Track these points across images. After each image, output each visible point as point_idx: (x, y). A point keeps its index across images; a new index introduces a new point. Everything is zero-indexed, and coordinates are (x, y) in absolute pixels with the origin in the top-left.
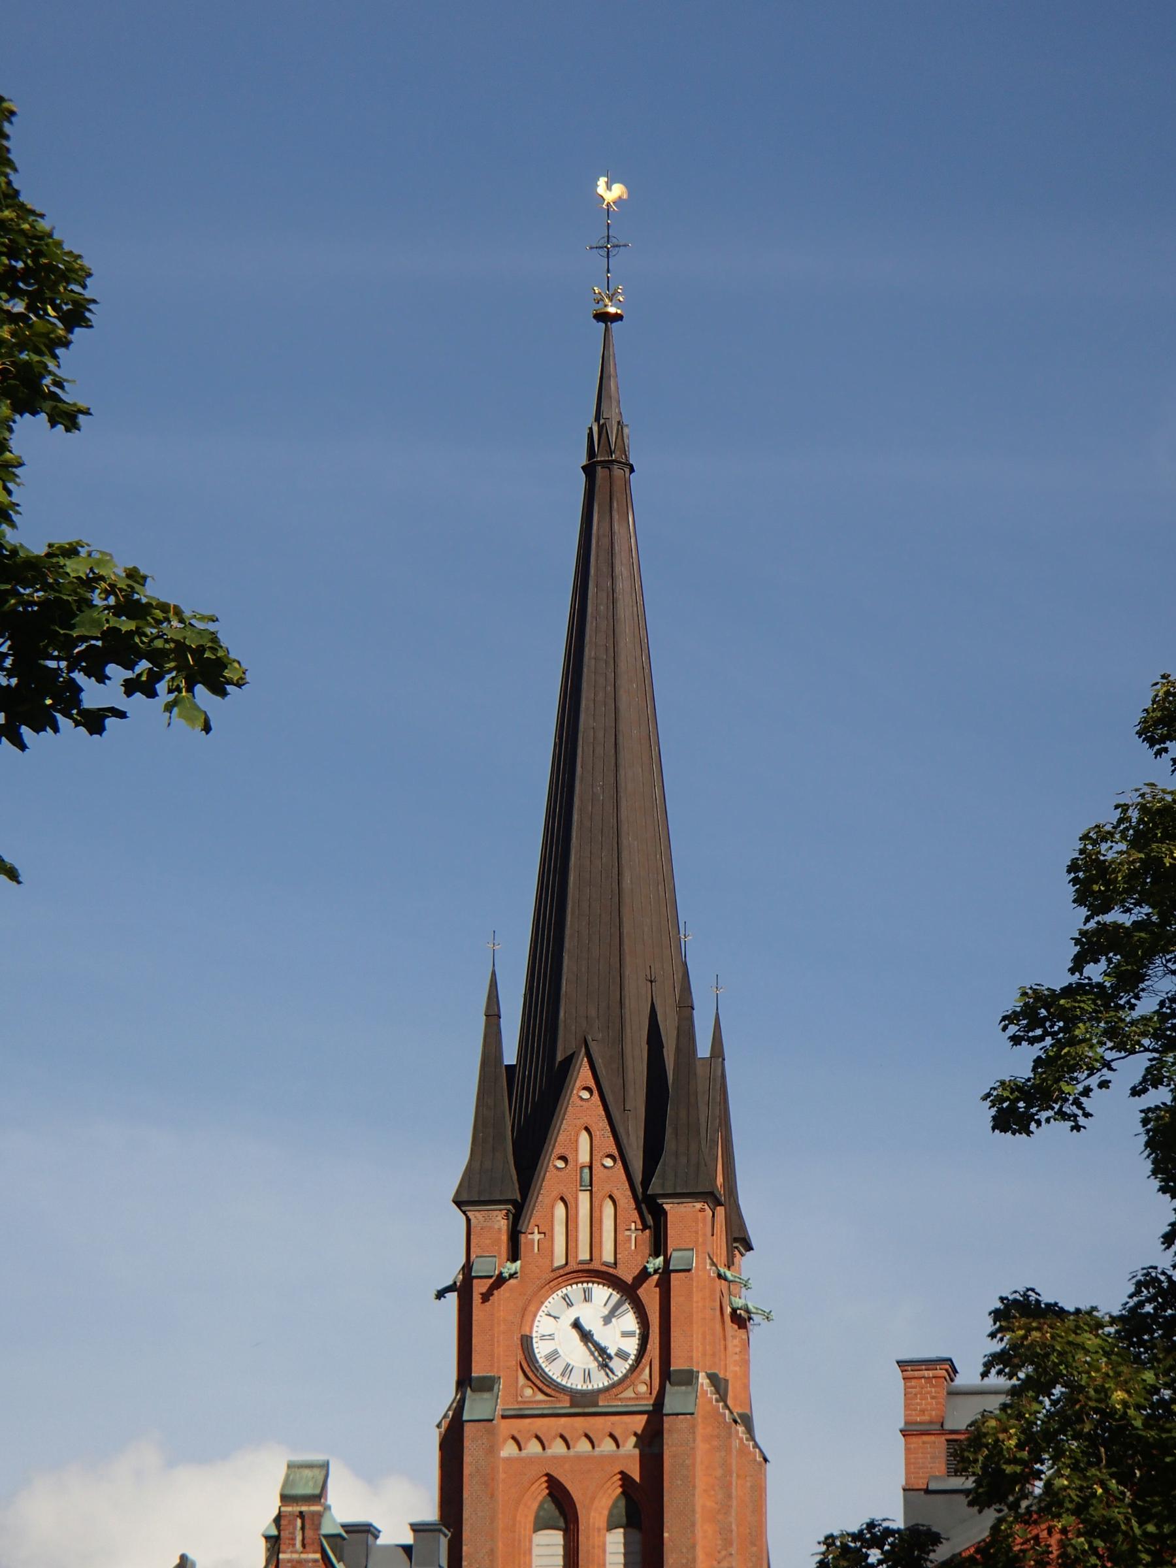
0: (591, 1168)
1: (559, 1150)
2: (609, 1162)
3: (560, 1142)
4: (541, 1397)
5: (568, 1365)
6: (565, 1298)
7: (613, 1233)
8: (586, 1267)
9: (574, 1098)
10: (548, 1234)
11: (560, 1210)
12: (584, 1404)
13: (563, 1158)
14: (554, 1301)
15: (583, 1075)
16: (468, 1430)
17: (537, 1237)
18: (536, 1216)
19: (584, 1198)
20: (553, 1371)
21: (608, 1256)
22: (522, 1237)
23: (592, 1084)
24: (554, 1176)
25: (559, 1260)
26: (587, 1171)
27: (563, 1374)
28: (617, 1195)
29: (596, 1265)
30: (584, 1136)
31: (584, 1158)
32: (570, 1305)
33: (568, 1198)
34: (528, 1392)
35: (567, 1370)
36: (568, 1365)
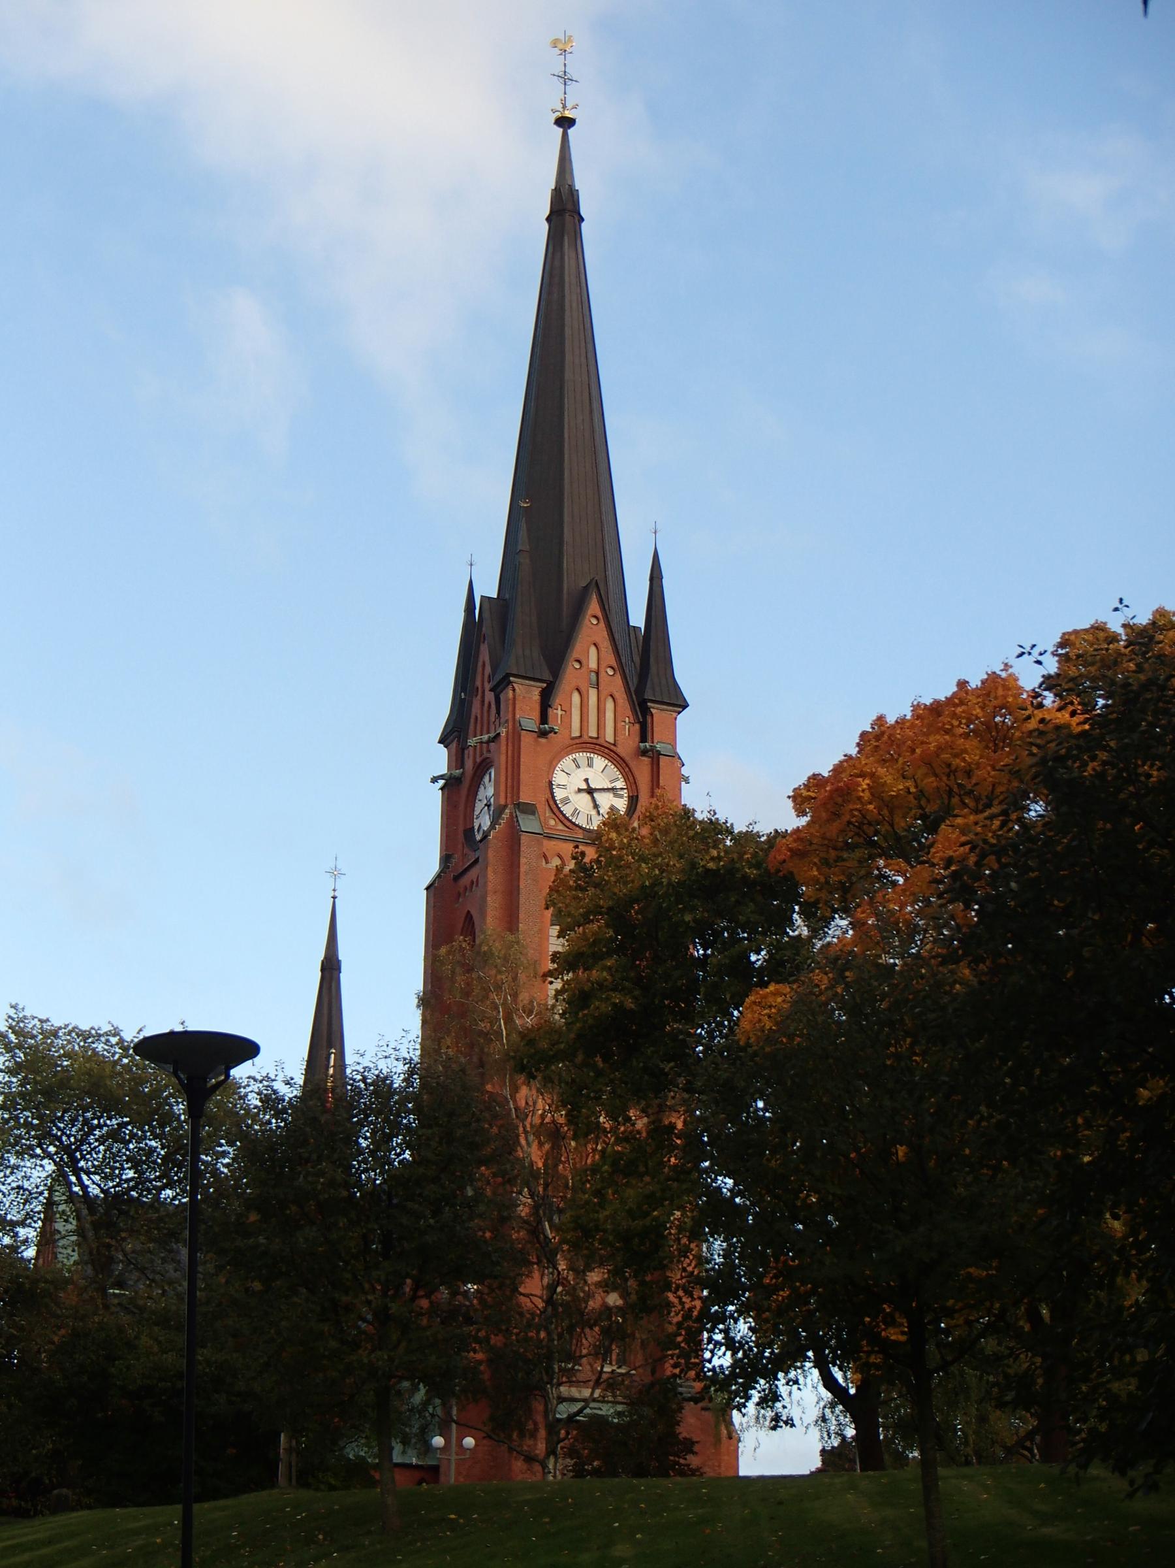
0: (597, 674)
2: (611, 672)
3: (577, 651)
4: (561, 827)
5: (576, 809)
6: (574, 760)
7: (612, 719)
8: (594, 741)
9: (586, 621)
10: (567, 712)
11: (576, 698)
13: (578, 661)
14: (567, 762)
15: (594, 607)
16: (524, 839)
17: (560, 712)
18: (558, 700)
19: (593, 693)
20: (567, 810)
21: (610, 738)
22: (550, 710)
23: (600, 615)
24: (571, 675)
25: (576, 733)
26: (593, 675)
27: (573, 815)
28: (617, 695)
29: (601, 741)
30: (593, 650)
31: (593, 665)
32: (578, 767)
33: (583, 689)
34: (552, 822)
35: (576, 812)
36: (576, 809)
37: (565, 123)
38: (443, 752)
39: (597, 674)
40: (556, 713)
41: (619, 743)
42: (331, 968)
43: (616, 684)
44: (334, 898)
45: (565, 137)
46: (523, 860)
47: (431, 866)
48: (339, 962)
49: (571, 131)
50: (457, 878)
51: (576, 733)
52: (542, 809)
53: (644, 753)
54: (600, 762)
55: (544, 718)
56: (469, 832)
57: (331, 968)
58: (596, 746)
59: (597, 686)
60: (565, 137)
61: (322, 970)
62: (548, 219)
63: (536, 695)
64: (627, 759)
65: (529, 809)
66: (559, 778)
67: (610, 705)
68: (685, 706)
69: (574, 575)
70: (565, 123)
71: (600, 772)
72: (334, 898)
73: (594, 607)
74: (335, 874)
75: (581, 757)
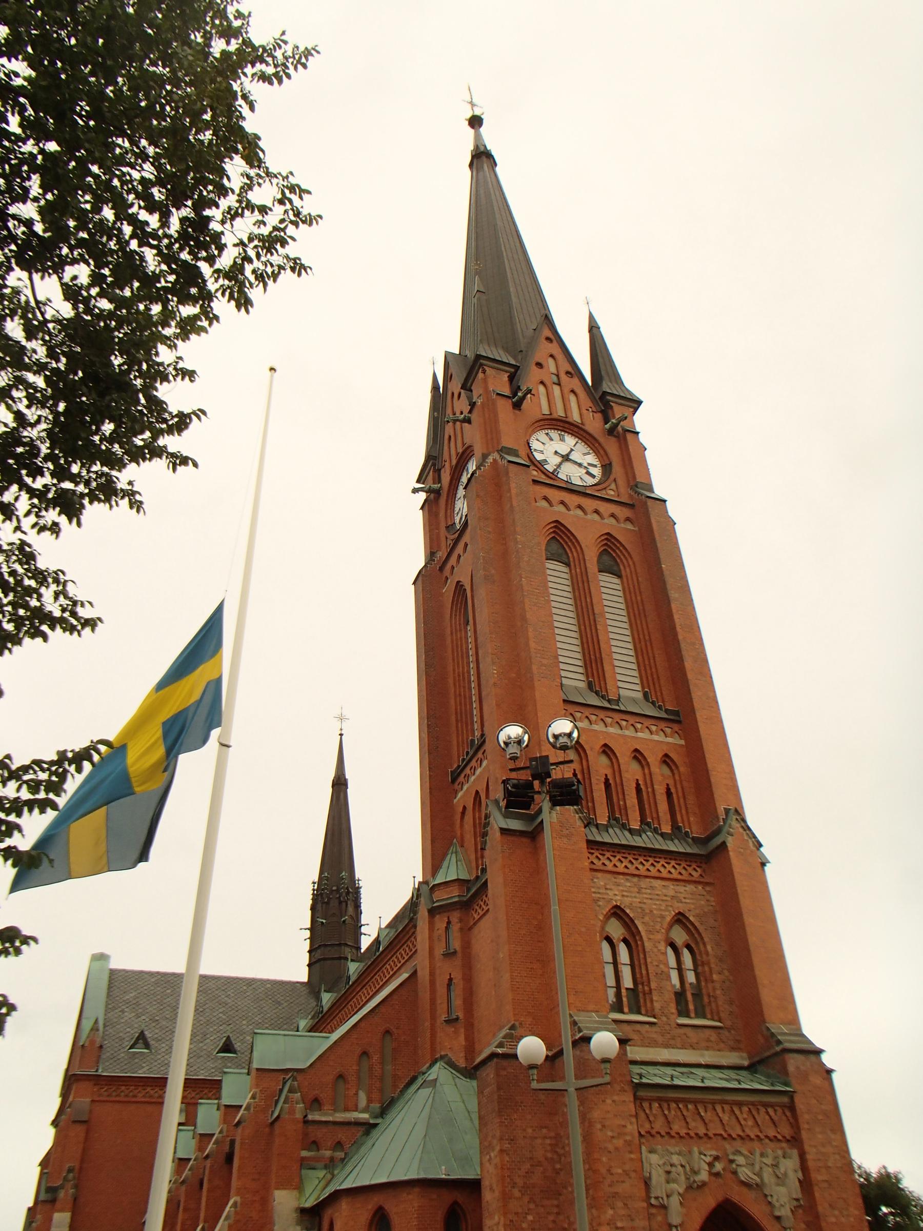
0: (558, 376)
25: (546, 410)
31: (553, 369)
37: (475, 122)
39: (558, 376)
41: (586, 422)
42: (340, 784)
44: (341, 735)
46: (513, 485)
47: (418, 560)
48: (346, 780)
49: (482, 130)
50: (441, 569)
51: (546, 410)
57: (340, 784)
59: (559, 384)
61: (333, 786)
62: (471, 165)
64: (596, 435)
66: (535, 445)
67: (572, 398)
68: (639, 403)
69: (525, 324)
72: (341, 735)
73: (547, 333)
74: (341, 719)
75: (554, 434)
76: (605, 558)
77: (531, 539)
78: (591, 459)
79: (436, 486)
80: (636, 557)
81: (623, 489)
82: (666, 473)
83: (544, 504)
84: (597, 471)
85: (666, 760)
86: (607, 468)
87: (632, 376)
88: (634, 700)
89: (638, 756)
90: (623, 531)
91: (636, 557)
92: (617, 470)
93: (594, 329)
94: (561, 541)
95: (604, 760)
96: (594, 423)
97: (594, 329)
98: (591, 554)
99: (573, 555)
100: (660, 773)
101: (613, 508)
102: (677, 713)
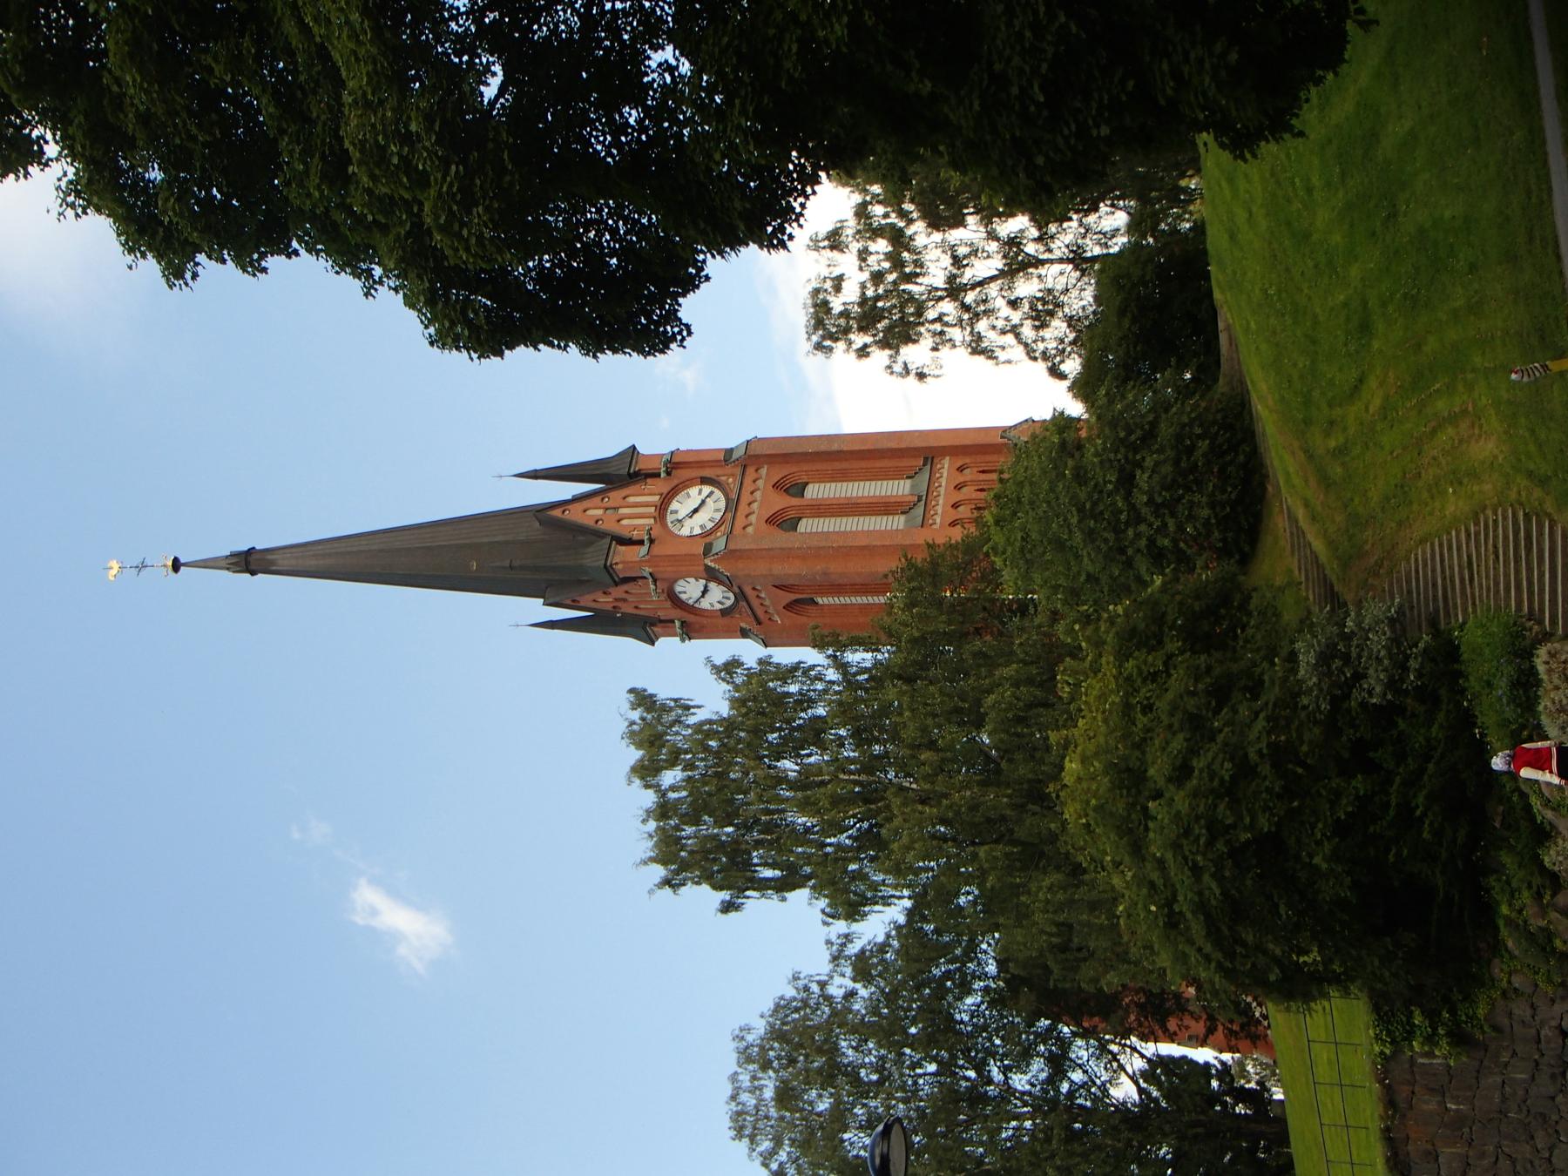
1: (591, 523)
11: (625, 522)
12: (732, 505)
16: (732, 546)
18: (626, 534)
20: (710, 525)
30: (590, 512)
31: (600, 512)
35: (711, 520)
38: (663, 642)
40: (636, 535)
43: (615, 497)
45: (185, 565)
52: (708, 540)
53: (668, 474)
54: (674, 505)
55: (641, 542)
56: (725, 612)
58: (662, 508)
60: (185, 565)
62: (253, 573)
63: (623, 548)
65: (708, 549)
67: (631, 499)
68: (634, 447)
70: (176, 565)
71: (681, 506)
73: (557, 513)
76: (792, 491)
77: (781, 539)
78: (694, 491)
79: (677, 623)
80: (794, 469)
81: (728, 469)
82: (727, 435)
83: (750, 529)
84: (707, 489)
85: (961, 469)
86: (705, 481)
87: (604, 447)
88: (912, 487)
89: (958, 487)
90: (765, 476)
91: (794, 469)
92: (707, 473)
93: (535, 475)
94: (784, 521)
95: (961, 509)
96: (661, 486)
97: (535, 475)
98: (795, 501)
99: (792, 514)
100: (968, 474)
101: (748, 480)
102: (926, 460)
